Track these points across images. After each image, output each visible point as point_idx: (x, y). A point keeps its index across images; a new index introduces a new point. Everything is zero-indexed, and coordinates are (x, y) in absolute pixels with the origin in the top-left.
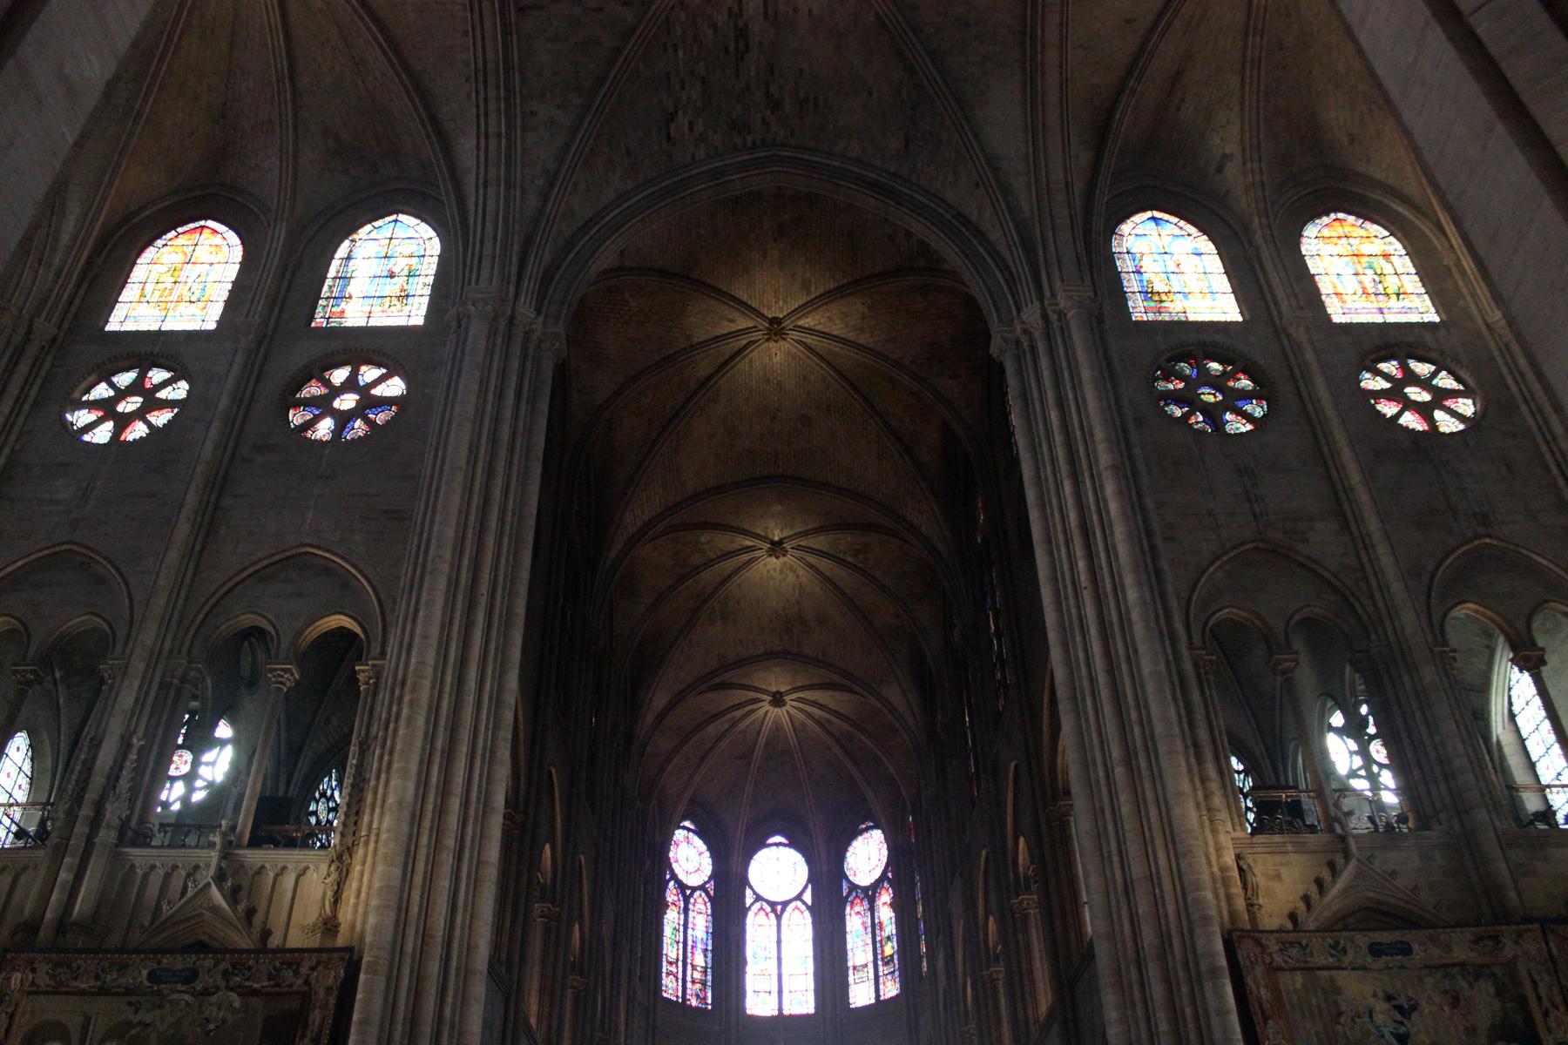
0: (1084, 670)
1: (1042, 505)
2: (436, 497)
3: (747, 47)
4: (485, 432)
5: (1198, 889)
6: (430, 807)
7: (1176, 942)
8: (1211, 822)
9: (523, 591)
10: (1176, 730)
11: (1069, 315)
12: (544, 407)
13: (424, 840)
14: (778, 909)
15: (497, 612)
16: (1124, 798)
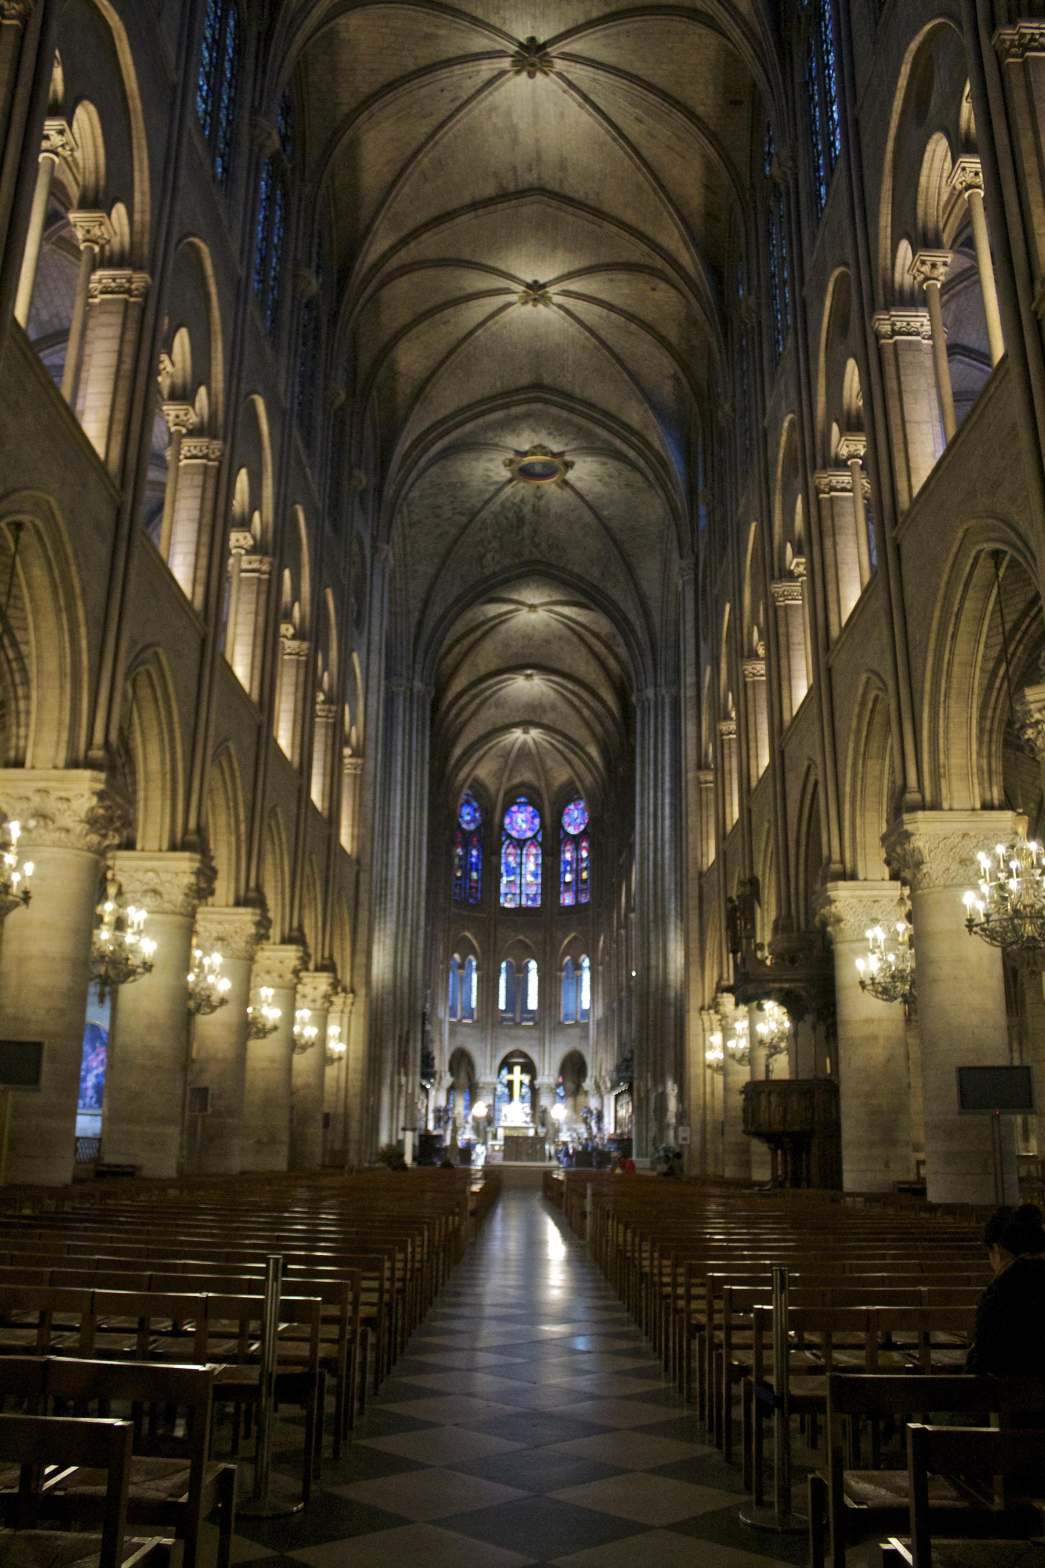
3: (523, 524)
12: (428, 733)
14: (520, 844)
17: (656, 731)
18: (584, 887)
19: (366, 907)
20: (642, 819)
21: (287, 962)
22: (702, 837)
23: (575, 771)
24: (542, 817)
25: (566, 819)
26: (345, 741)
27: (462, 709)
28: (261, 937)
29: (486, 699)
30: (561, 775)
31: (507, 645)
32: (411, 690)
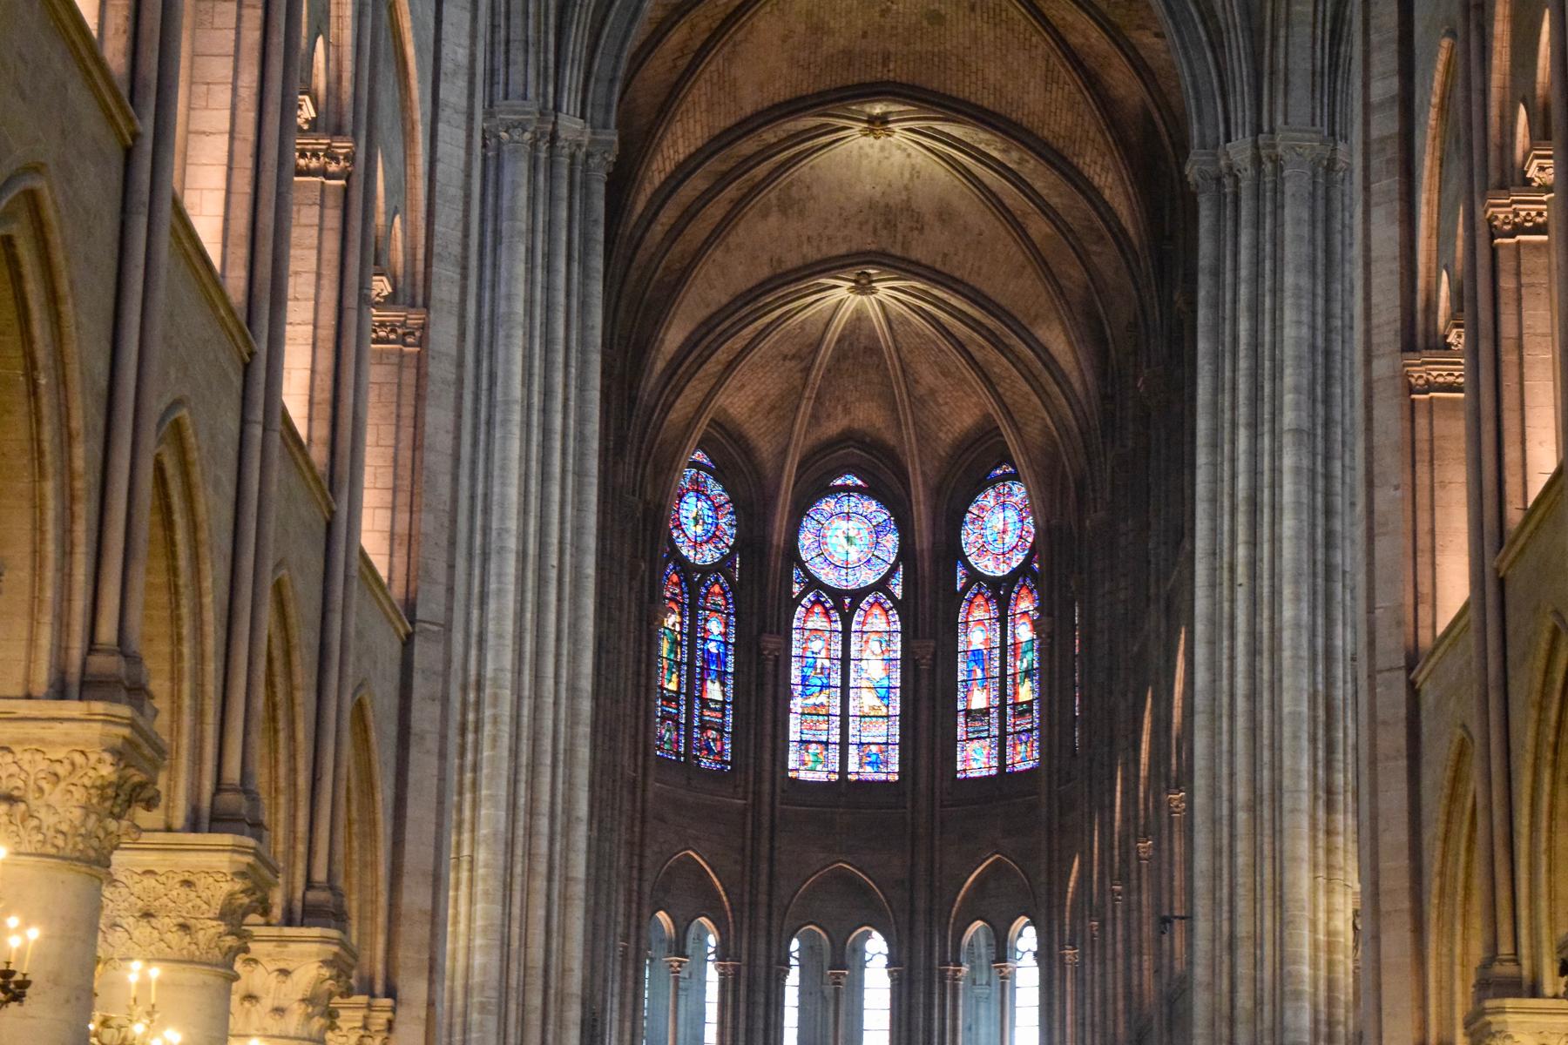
0: (1225, 682)
1: (1215, 446)
2: (489, 434)
4: (537, 333)
5: (1295, 963)
6: (520, 832)
7: (1267, 1008)
8: (1329, 880)
9: (591, 542)
10: (1305, 784)
11: (1286, 173)
12: (598, 263)
13: (518, 869)
14: (844, 603)
15: (567, 579)
16: (1242, 846)
17: (1257, 262)
18: (1024, 724)
19: (432, 743)
20: (1214, 517)
21: (202, 882)
22: (1420, 550)
23: (999, 398)
24: (903, 524)
25: (969, 538)
26: (376, 259)
27: (689, 214)
28: (128, 795)
29: (756, 188)
30: (961, 411)
31: (817, 29)
32: (554, 137)
